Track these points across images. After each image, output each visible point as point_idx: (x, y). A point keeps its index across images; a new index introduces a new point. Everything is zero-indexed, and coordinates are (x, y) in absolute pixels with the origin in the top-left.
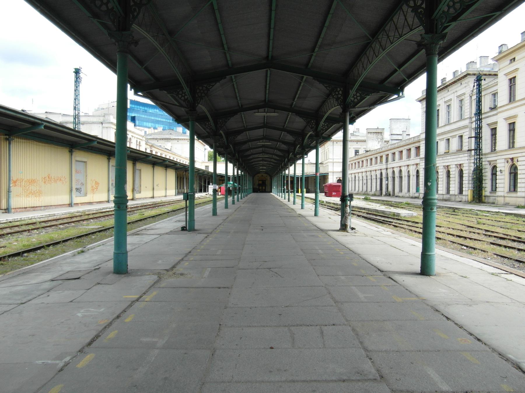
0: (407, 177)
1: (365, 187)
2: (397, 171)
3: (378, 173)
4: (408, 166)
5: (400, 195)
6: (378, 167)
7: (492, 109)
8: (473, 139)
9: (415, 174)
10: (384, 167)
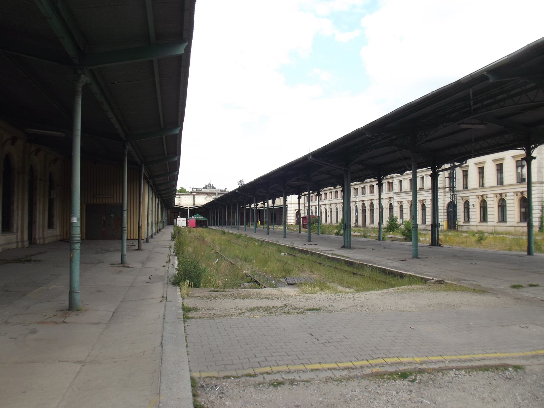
8: (447, 179)
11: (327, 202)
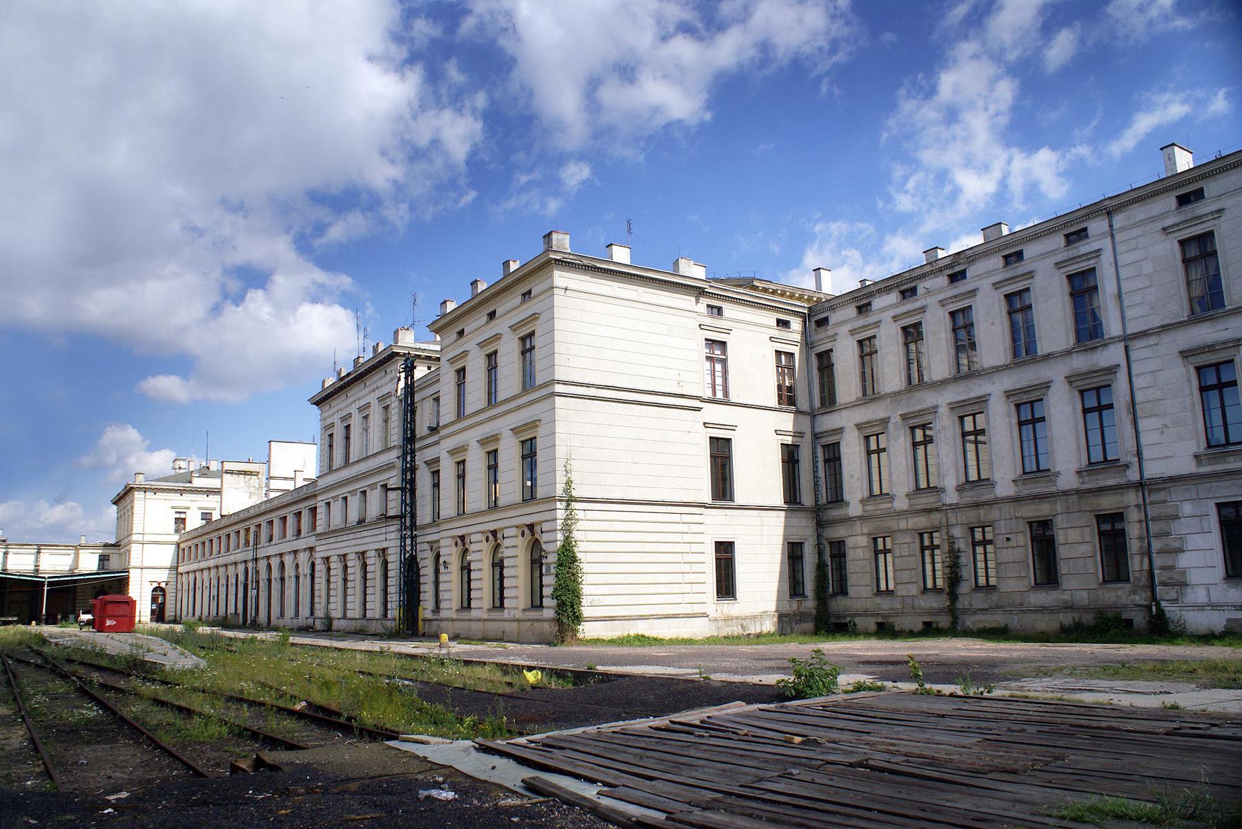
0: (293, 579)
1: (214, 604)
2: (275, 562)
3: (241, 568)
4: (295, 552)
5: (281, 623)
6: (239, 557)
7: (434, 430)
9: (308, 571)
10: (250, 556)
11: (212, 563)
